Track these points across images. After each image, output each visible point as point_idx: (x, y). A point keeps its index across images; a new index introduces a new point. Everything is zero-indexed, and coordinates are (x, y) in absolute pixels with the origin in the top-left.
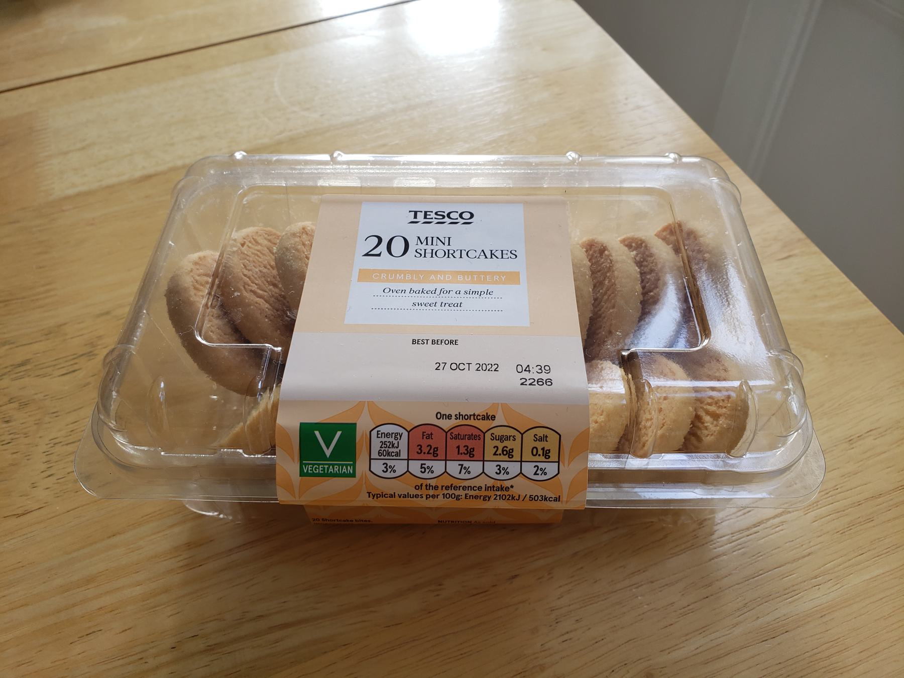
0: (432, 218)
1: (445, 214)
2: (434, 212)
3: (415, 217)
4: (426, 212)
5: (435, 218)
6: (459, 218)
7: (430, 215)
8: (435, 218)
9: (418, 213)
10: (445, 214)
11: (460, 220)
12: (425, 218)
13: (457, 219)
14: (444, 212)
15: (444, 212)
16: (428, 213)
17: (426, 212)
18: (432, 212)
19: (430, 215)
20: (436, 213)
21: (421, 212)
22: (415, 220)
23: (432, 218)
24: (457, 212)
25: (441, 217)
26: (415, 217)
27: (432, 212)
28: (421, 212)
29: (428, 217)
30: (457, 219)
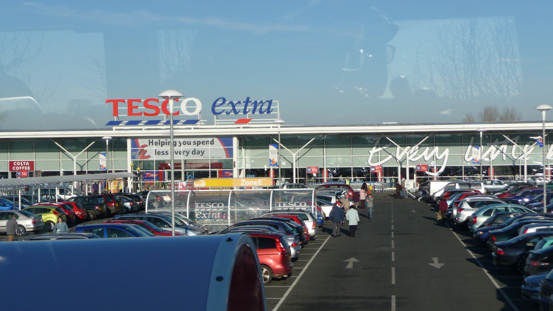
3: (116, 113)
4: (130, 102)
5: (146, 114)
8: (146, 114)
9: (119, 103)
12: (130, 113)
17: (130, 102)
18: (139, 101)
19: (137, 107)
20: (146, 104)
21: (123, 101)
22: (115, 119)
23: (140, 114)
25: (153, 111)
26: (116, 113)
27: (139, 101)
28: (123, 101)
29: (135, 111)
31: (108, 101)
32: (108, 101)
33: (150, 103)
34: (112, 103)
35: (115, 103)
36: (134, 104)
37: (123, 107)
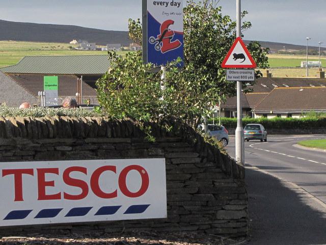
0: (57, 197)
1: (87, 179)
2: (61, 172)
3: (19, 197)
5: (67, 197)
6: (120, 193)
7: (51, 184)
8: (67, 197)
9: (23, 175)
10: (87, 179)
11: (124, 202)
12: (42, 196)
13: (114, 195)
14: (84, 170)
15: (84, 170)
16: (48, 177)
17: (42, 172)
18: (55, 171)
19: (51, 184)
20: (68, 181)
21: (30, 172)
22: (19, 206)
23: (57, 197)
24: (113, 169)
25: (78, 191)
26: (19, 197)
27: (55, 171)
28: (30, 172)
30: (114, 195)
31: (6, 172)
32: (6, 172)
33: (73, 175)
34: (13, 176)
35: (18, 174)
36: (48, 177)
37: (30, 183)
